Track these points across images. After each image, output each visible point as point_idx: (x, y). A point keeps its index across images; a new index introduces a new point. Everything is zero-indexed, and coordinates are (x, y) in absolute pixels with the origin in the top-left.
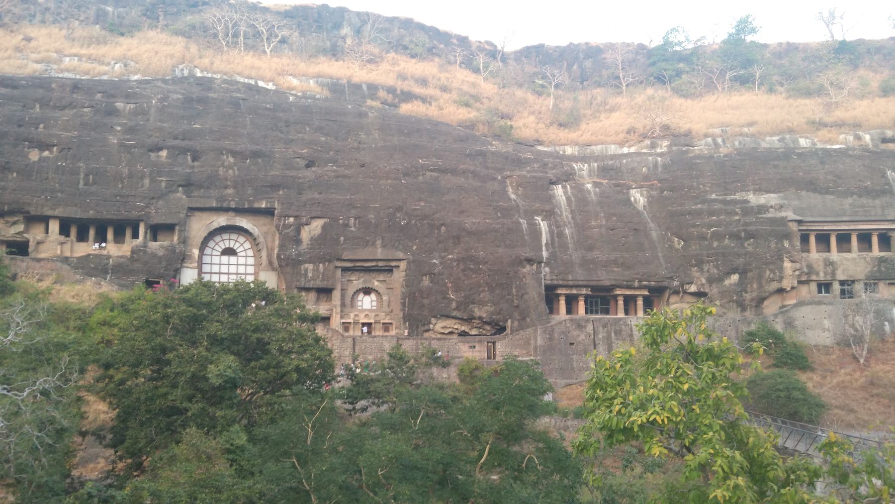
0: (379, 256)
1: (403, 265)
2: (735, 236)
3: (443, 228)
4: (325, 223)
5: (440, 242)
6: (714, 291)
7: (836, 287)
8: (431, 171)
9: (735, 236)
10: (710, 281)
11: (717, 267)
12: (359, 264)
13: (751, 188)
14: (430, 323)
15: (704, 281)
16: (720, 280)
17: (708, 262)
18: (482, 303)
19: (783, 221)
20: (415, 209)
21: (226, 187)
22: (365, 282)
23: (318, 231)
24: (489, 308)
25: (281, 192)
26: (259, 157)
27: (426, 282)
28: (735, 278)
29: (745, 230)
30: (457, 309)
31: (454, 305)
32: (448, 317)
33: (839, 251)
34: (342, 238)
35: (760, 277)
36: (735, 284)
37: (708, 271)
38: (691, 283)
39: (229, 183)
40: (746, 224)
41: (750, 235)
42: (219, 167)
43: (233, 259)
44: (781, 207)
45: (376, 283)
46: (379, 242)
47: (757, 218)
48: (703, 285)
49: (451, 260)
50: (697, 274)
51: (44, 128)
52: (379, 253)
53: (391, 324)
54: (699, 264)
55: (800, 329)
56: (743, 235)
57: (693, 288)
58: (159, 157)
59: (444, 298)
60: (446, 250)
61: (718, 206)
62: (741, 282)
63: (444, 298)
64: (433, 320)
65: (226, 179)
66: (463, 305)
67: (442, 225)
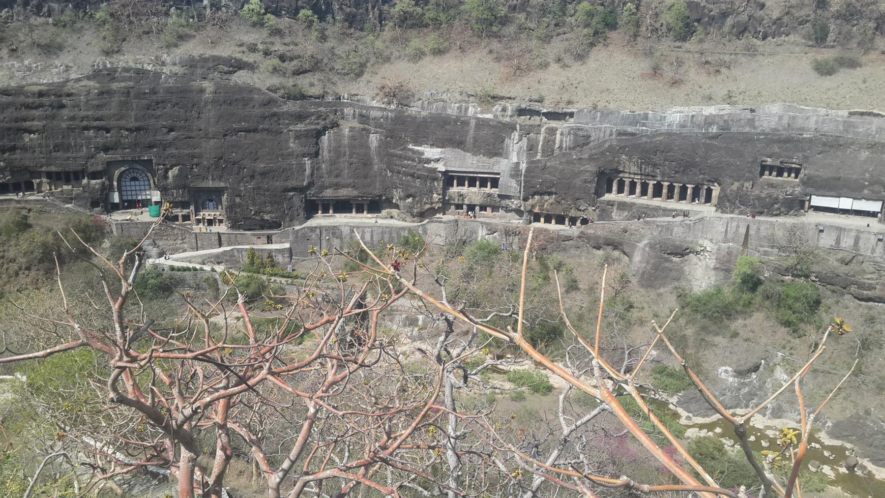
6: (401, 204)
9: (412, 175)
19: (434, 170)
28: (410, 200)
43: (137, 183)
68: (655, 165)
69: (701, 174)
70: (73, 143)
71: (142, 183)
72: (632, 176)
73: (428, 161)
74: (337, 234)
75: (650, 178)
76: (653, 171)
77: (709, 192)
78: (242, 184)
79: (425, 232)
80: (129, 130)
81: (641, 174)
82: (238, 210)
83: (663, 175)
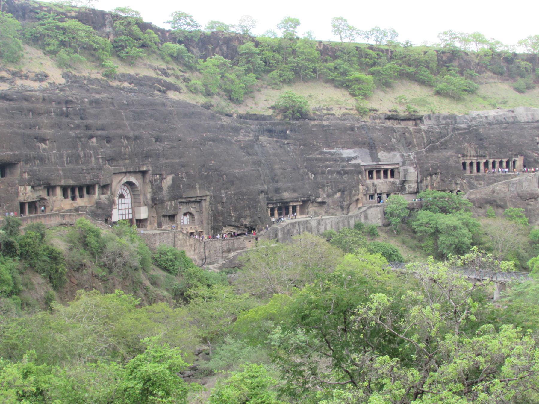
0: (199, 195)
1: (208, 199)
2: (339, 173)
3: (225, 176)
4: (173, 177)
5: (224, 184)
6: (330, 201)
7: (376, 196)
8: (210, 141)
9: (339, 173)
10: (328, 196)
11: (332, 189)
12: (188, 199)
13: (340, 145)
14: (222, 230)
15: (325, 196)
16: (333, 195)
17: (327, 186)
18: (245, 218)
19: (358, 166)
20: (210, 166)
21: (126, 159)
22: (187, 209)
23: (170, 183)
24: (249, 219)
25: (150, 160)
26: (138, 139)
27: (220, 208)
28: (338, 195)
29: (343, 170)
30: (235, 221)
31: (233, 219)
32: (230, 225)
33: (377, 179)
34: (181, 186)
35: (350, 193)
36: (339, 197)
37: (327, 191)
38: (319, 197)
39: (127, 156)
40: (344, 167)
41: (346, 173)
42: (122, 147)
43: (123, 200)
44: (355, 158)
45: (192, 209)
46: (197, 186)
47: (348, 164)
48: (324, 198)
49: (231, 194)
50: (321, 193)
51: (39, 129)
52: (198, 193)
53: (202, 232)
54: (323, 186)
55: (370, 219)
56: (342, 172)
57: (319, 200)
58: (92, 142)
59: (229, 215)
60: (227, 188)
61: (328, 156)
62: (342, 196)
63: (229, 215)
64: (224, 228)
65: (125, 154)
66: (238, 219)
67: (225, 174)
68: (485, 148)
69: (510, 151)
70: (82, 154)
71: (126, 200)
72: (472, 158)
73: (350, 159)
74: (309, 228)
75: (482, 158)
76: (484, 153)
77: (514, 162)
78: (223, 191)
79: (366, 217)
80: (128, 138)
81: (477, 156)
82: (221, 218)
83: (490, 154)
